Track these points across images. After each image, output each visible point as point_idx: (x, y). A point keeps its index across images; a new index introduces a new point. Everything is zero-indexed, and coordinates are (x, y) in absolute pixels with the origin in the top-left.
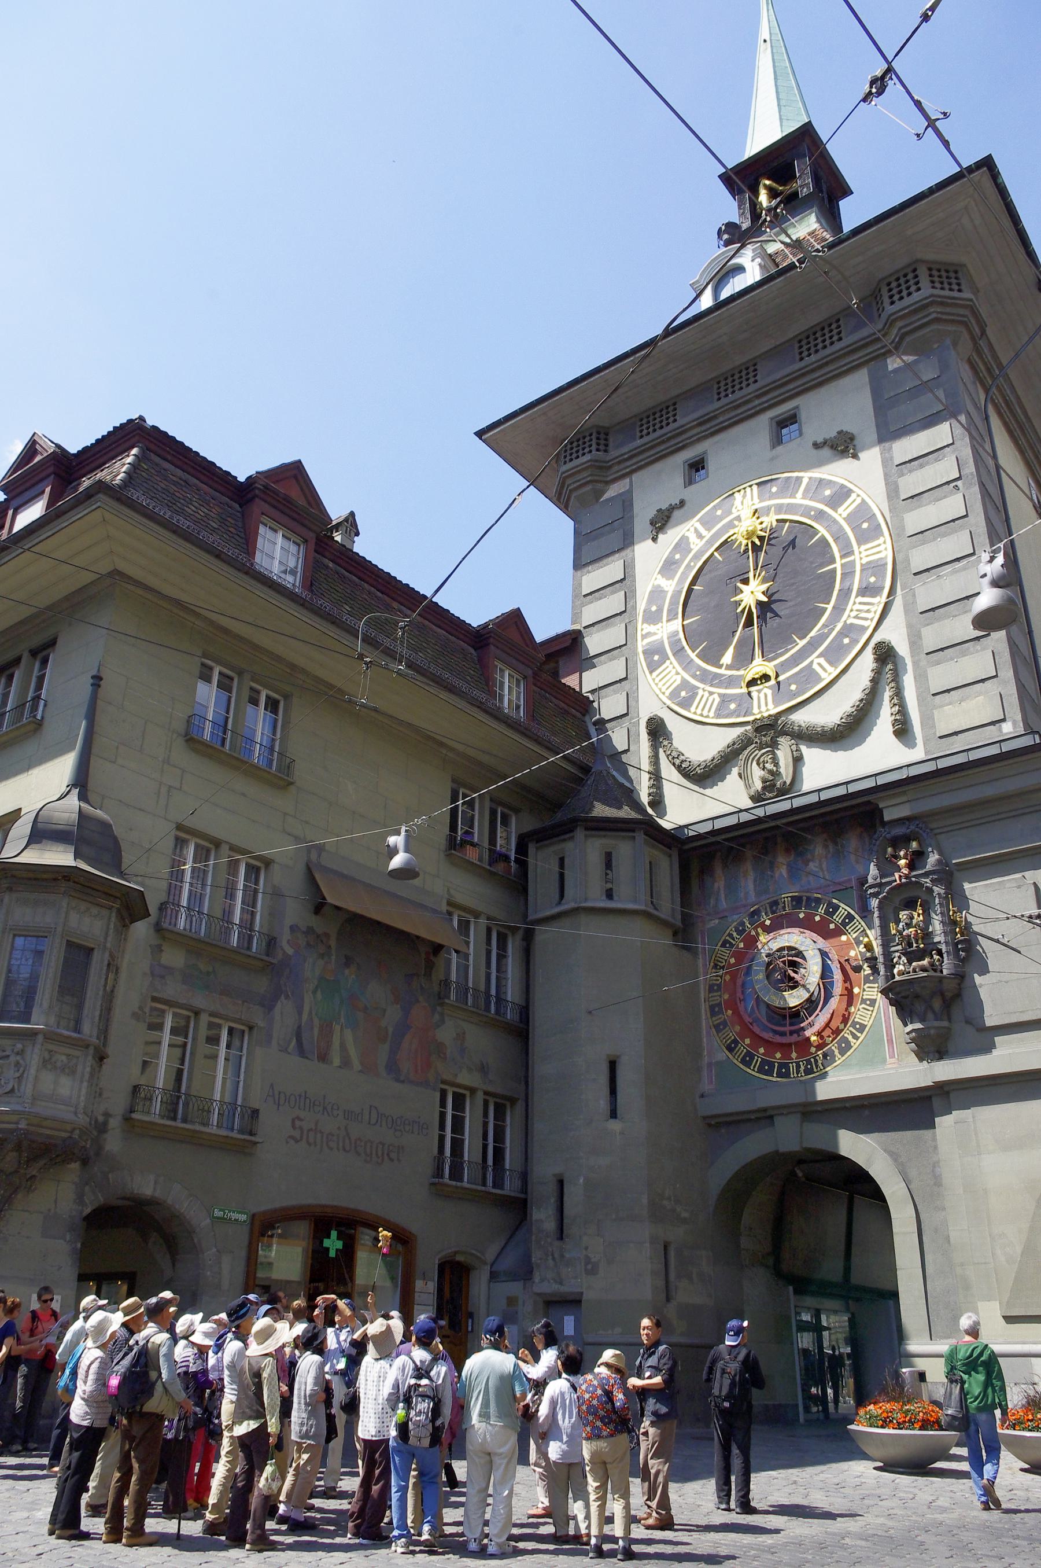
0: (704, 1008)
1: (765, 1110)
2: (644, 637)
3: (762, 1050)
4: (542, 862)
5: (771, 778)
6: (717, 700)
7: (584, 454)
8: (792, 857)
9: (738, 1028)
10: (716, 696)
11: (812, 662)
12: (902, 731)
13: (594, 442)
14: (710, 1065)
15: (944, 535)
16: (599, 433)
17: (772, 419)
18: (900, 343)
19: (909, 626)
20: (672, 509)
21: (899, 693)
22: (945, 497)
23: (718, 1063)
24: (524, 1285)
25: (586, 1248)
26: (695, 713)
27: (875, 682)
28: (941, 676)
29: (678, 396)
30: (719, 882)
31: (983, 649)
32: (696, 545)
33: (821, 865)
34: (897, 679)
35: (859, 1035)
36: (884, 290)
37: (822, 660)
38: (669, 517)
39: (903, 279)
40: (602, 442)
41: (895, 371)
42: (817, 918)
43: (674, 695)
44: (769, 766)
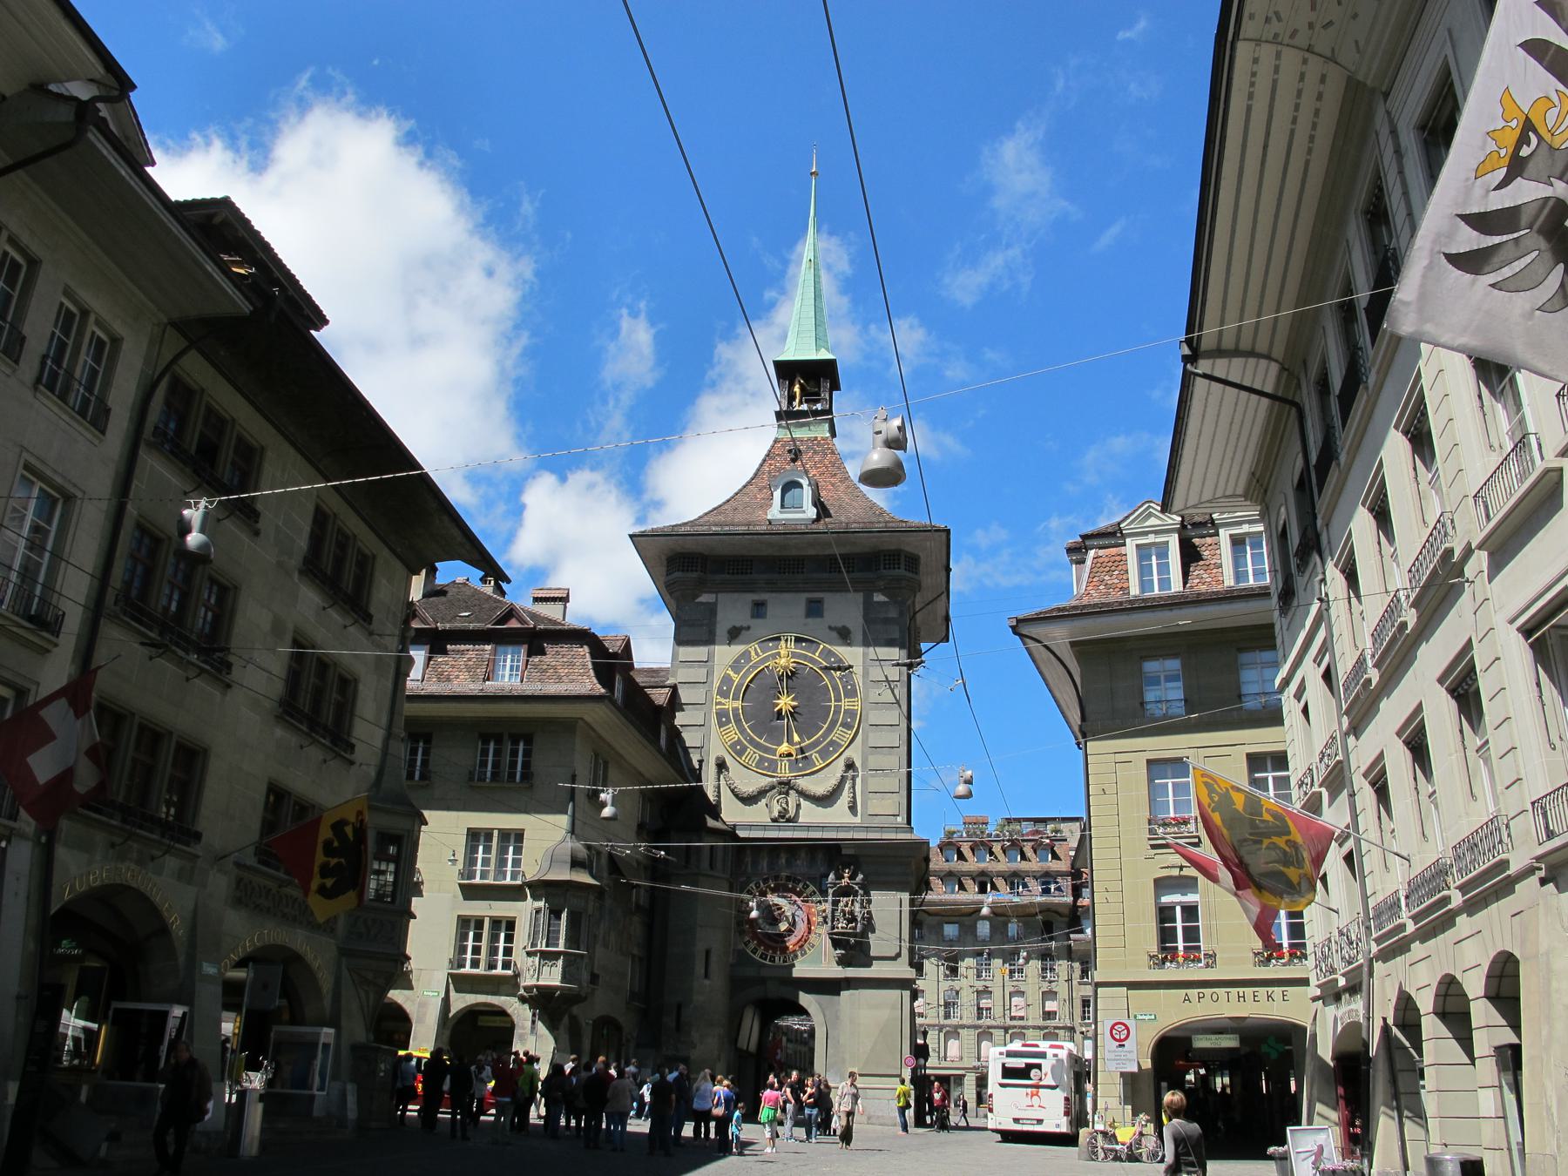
12: (853, 808)
21: (854, 787)
34: (854, 779)
43: (733, 746)
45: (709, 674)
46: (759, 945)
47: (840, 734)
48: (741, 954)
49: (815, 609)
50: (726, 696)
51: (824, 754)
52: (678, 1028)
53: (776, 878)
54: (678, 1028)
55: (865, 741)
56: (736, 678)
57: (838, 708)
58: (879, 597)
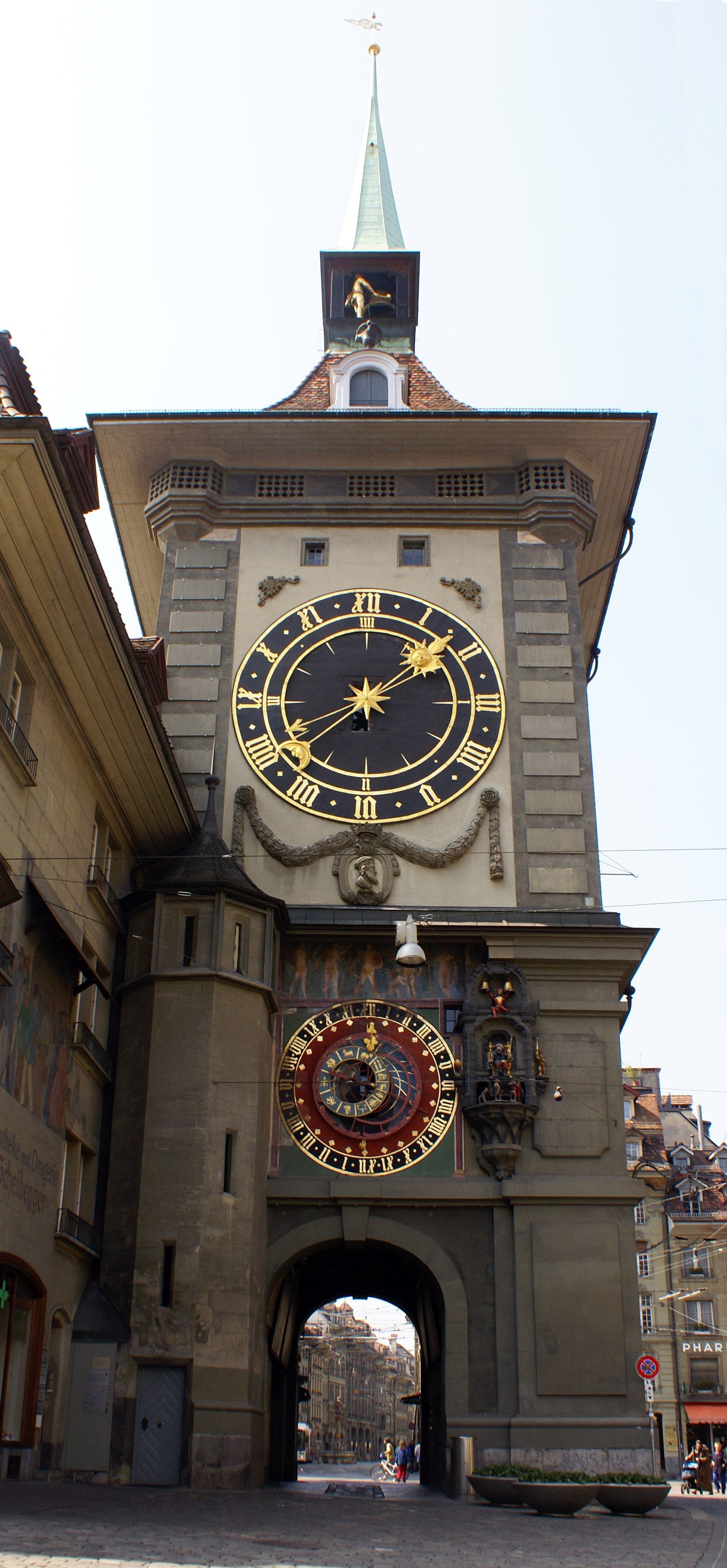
0: (273, 1092)
1: (335, 1199)
2: (239, 701)
3: (332, 1143)
4: (168, 917)
5: (369, 885)
6: (317, 791)
7: (196, 486)
8: (381, 966)
9: (308, 1118)
10: (316, 787)
11: (419, 786)
13: (210, 478)
14: (274, 1148)
15: (553, 714)
16: (215, 471)
17: (401, 537)
18: (533, 524)
19: (514, 784)
20: (284, 582)
22: (557, 680)
23: (282, 1147)
24: (119, 1347)
25: (198, 1317)
26: (291, 797)
27: (479, 825)
28: (537, 839)
29: (306, 471)
30: (301, 974)
31: (576, 827)
32: (308, 628)
33: (409, 980)
35: (431, 1143)
36: (532, 472)
37: (429, 788)
38: (280, 588)
39: (553, 472)
40: (217, 481)
41: (525, 546)
42: (401, 1030)
43: (270, 772)
44: (370, 874)
45: (227, 652)
46: (325, 1137)
47: (467, 752)
48: (292, 1160)
49: (413, 552)
50: (256, 687)
51: (443, 787)
52: (167, 1298)
53: (357, 1008)
54: (167, 1298)
55: (516, 766)
56: (275, 659)
57: (464, 711)
58: (526, 538)
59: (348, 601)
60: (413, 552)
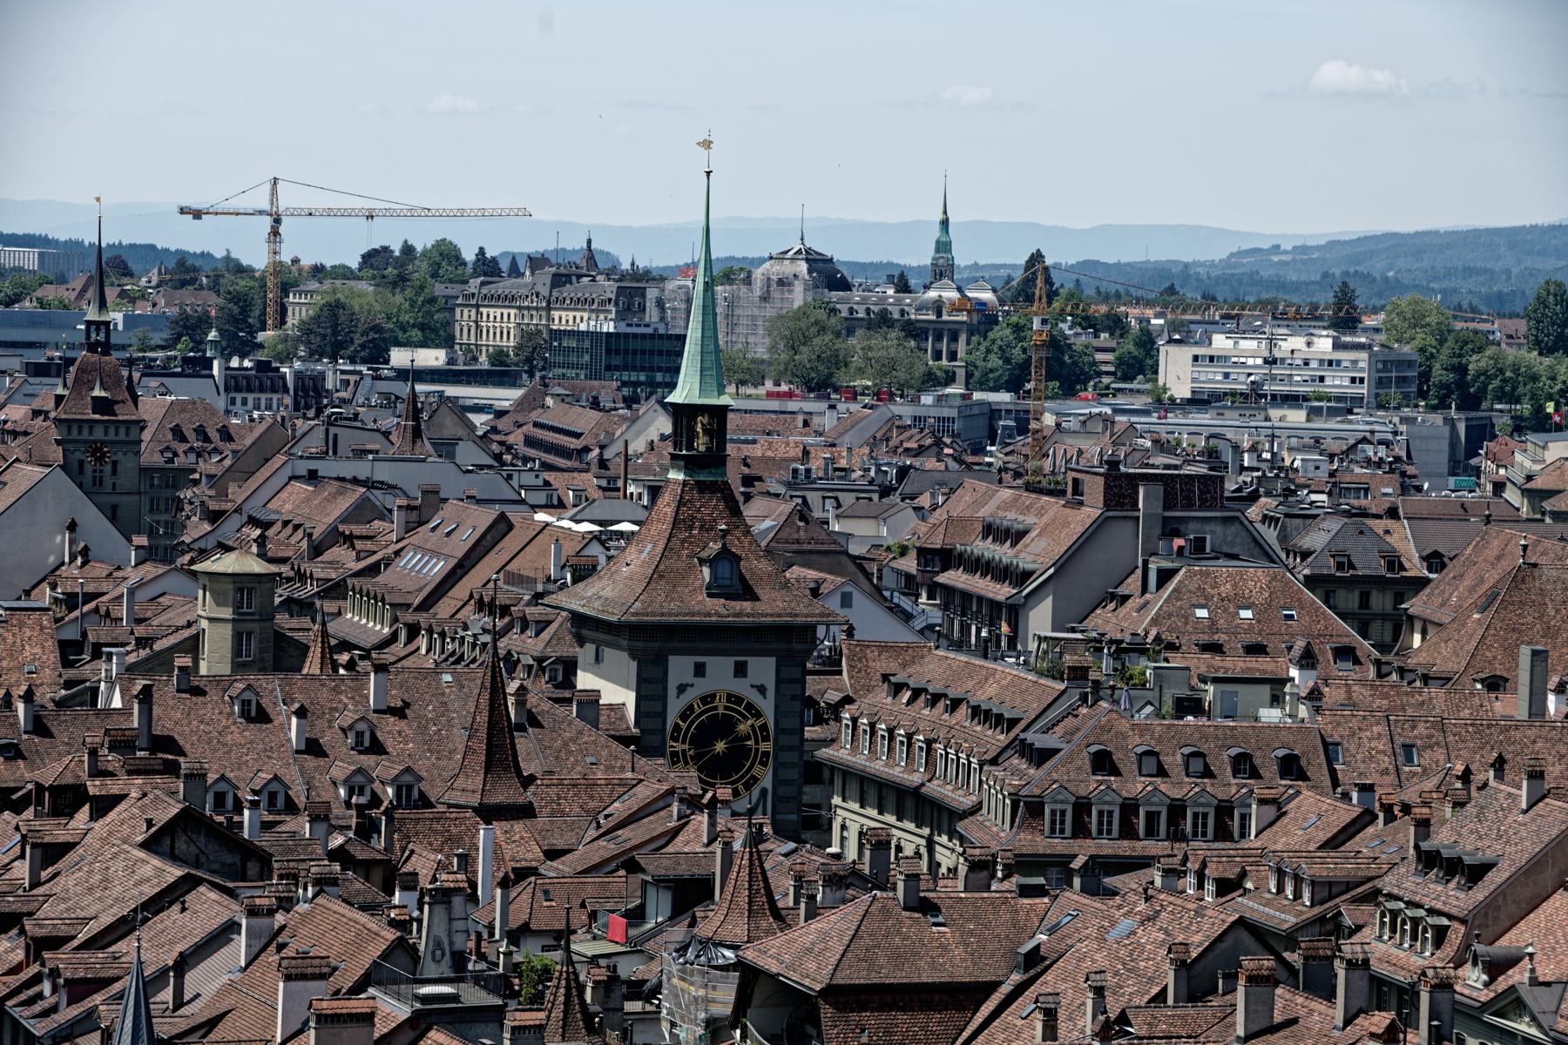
32: (697, 711)
45: (664, 722)
47: (757, 770)
49: (740, 670)
56: (684, 726)
59: (713, 696)
60: (740, 670)
